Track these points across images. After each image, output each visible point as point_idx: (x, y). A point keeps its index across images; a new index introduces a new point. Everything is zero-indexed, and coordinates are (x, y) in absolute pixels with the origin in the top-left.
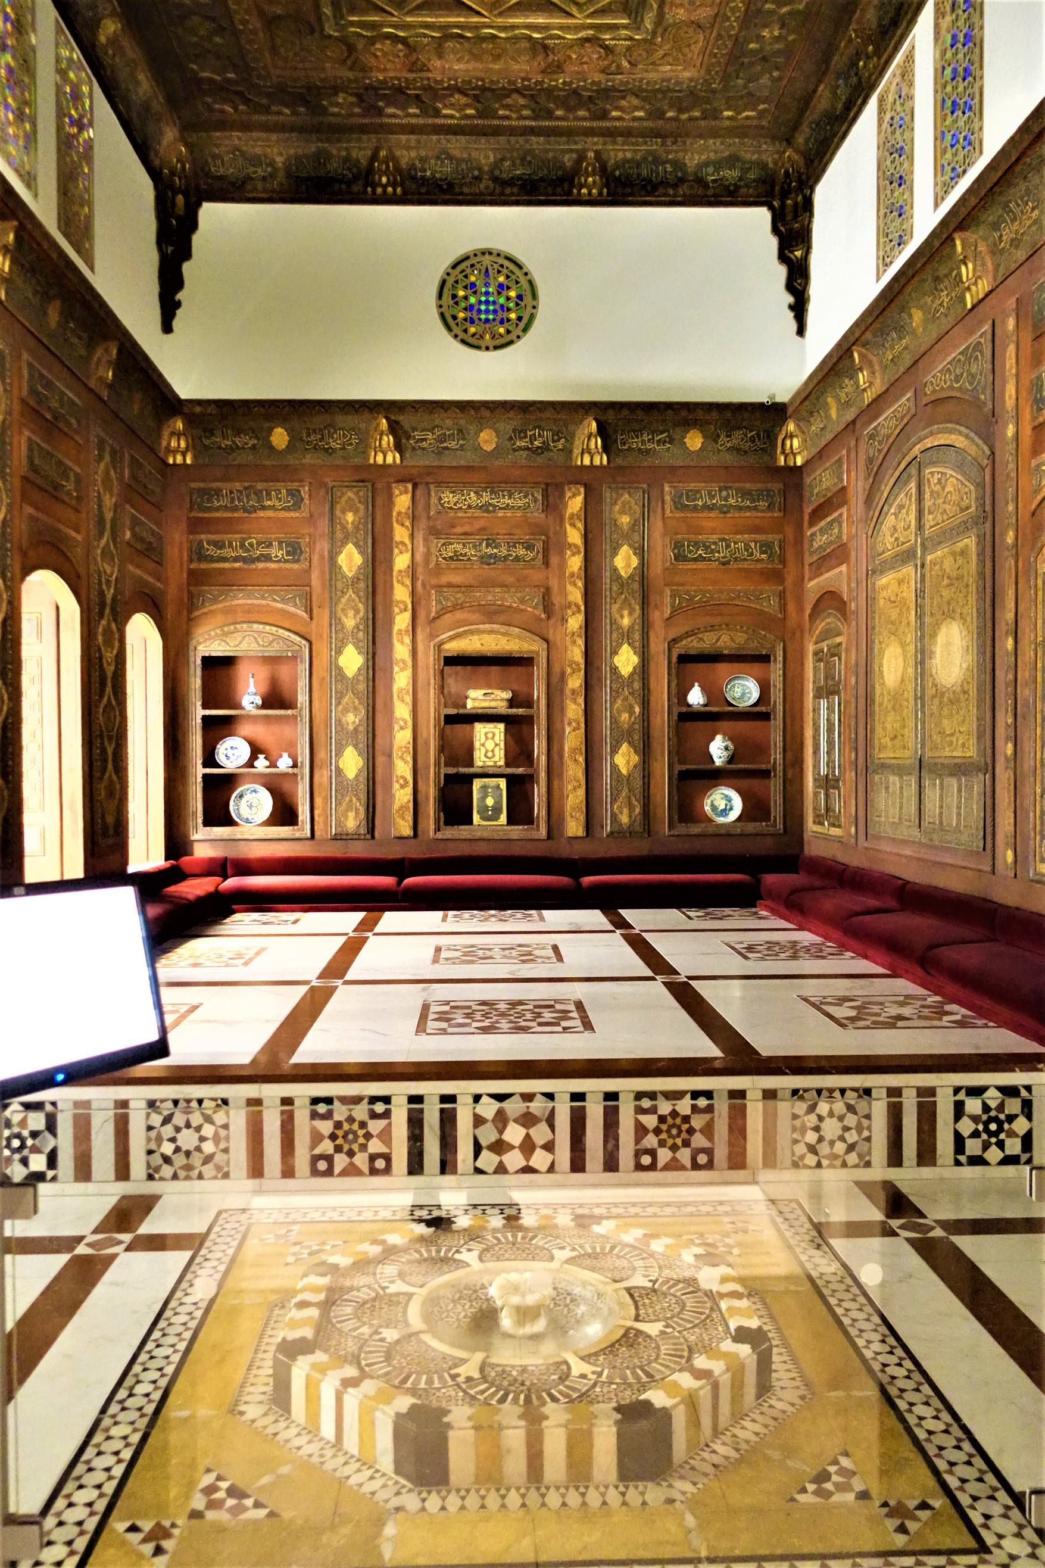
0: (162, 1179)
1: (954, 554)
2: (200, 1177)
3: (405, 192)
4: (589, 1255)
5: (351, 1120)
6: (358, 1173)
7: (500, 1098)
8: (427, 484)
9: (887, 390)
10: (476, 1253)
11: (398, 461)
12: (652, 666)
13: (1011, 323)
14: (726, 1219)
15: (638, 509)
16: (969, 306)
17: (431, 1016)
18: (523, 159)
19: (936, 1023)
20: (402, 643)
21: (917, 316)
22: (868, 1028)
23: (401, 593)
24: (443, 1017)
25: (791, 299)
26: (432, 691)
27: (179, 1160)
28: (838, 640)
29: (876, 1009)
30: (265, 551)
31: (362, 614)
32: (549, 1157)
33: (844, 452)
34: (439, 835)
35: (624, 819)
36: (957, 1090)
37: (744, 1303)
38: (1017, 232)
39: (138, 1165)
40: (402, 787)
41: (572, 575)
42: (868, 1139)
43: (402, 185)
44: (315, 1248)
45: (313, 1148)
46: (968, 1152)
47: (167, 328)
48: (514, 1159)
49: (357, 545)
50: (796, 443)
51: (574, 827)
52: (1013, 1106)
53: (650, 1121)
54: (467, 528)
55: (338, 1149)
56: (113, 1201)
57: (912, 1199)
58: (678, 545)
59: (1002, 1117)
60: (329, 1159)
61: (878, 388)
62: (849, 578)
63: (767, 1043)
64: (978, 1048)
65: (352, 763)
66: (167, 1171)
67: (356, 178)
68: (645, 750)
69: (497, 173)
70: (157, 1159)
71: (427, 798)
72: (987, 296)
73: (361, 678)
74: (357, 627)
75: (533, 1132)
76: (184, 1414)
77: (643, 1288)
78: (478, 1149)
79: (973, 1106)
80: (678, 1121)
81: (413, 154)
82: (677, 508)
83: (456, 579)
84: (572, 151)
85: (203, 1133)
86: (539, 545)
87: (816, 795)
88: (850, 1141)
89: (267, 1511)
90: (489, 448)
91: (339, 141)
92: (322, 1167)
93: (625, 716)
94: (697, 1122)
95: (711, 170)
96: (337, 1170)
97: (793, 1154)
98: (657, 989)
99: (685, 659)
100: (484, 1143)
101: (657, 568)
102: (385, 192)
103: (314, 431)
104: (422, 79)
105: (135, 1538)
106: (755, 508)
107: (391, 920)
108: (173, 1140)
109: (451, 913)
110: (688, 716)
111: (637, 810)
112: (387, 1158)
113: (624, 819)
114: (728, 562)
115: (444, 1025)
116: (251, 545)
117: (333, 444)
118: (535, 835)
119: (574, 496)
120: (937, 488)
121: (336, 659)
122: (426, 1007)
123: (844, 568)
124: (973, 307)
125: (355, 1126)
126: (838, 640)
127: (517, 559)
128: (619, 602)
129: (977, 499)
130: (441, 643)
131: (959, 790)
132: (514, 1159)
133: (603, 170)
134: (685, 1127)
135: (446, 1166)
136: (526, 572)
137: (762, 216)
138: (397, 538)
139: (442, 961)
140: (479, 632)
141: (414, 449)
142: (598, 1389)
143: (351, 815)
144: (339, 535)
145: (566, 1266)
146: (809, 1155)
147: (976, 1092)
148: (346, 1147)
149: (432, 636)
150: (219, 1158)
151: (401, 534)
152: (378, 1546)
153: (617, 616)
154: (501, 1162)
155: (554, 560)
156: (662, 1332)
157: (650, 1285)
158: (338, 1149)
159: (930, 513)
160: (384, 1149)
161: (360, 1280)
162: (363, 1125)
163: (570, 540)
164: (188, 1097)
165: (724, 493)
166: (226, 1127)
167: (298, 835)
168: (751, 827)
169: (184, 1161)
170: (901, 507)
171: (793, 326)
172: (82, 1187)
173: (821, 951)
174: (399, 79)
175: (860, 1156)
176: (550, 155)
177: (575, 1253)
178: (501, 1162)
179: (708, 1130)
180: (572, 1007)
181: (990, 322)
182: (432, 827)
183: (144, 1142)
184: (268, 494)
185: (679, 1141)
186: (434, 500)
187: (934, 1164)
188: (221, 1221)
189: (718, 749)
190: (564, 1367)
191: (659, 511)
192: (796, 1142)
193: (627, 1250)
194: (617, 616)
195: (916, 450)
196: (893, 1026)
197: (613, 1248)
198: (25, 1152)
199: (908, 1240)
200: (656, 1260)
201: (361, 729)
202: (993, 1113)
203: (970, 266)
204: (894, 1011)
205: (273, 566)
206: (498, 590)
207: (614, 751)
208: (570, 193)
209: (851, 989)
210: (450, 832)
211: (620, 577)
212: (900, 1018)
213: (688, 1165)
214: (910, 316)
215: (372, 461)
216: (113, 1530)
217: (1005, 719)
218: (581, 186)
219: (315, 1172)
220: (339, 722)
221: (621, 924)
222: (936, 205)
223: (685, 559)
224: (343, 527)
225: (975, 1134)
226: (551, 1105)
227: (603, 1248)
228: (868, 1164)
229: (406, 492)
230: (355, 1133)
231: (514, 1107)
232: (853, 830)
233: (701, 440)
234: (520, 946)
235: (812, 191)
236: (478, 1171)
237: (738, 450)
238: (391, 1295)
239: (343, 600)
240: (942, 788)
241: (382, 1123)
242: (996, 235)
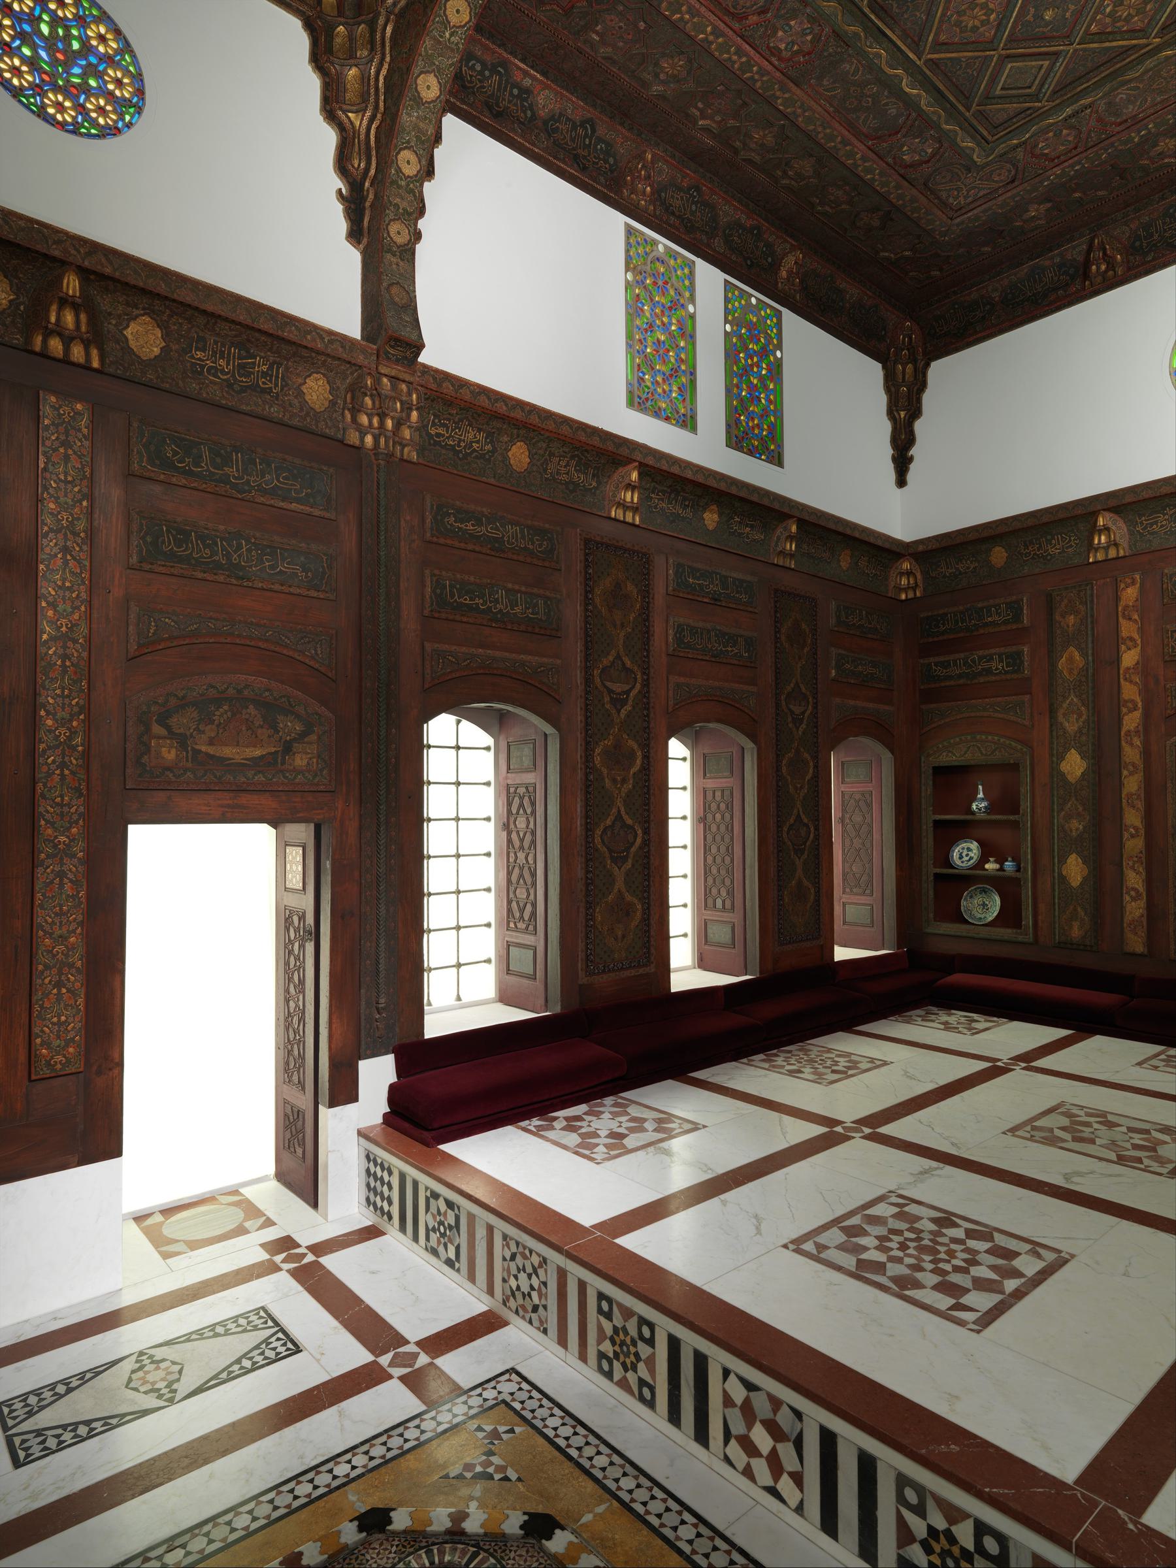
31: (1084, 717)
40: (1134, 899)
47: (901, 482)
65: (1075, 870)
74: (1080, 730)
116: (973, 661)
138: (1124, 633)
143: (1076, 925)
167: (1020, 938)
174: (1079, 163)
205: (994, 678)
239: (1065, 705)
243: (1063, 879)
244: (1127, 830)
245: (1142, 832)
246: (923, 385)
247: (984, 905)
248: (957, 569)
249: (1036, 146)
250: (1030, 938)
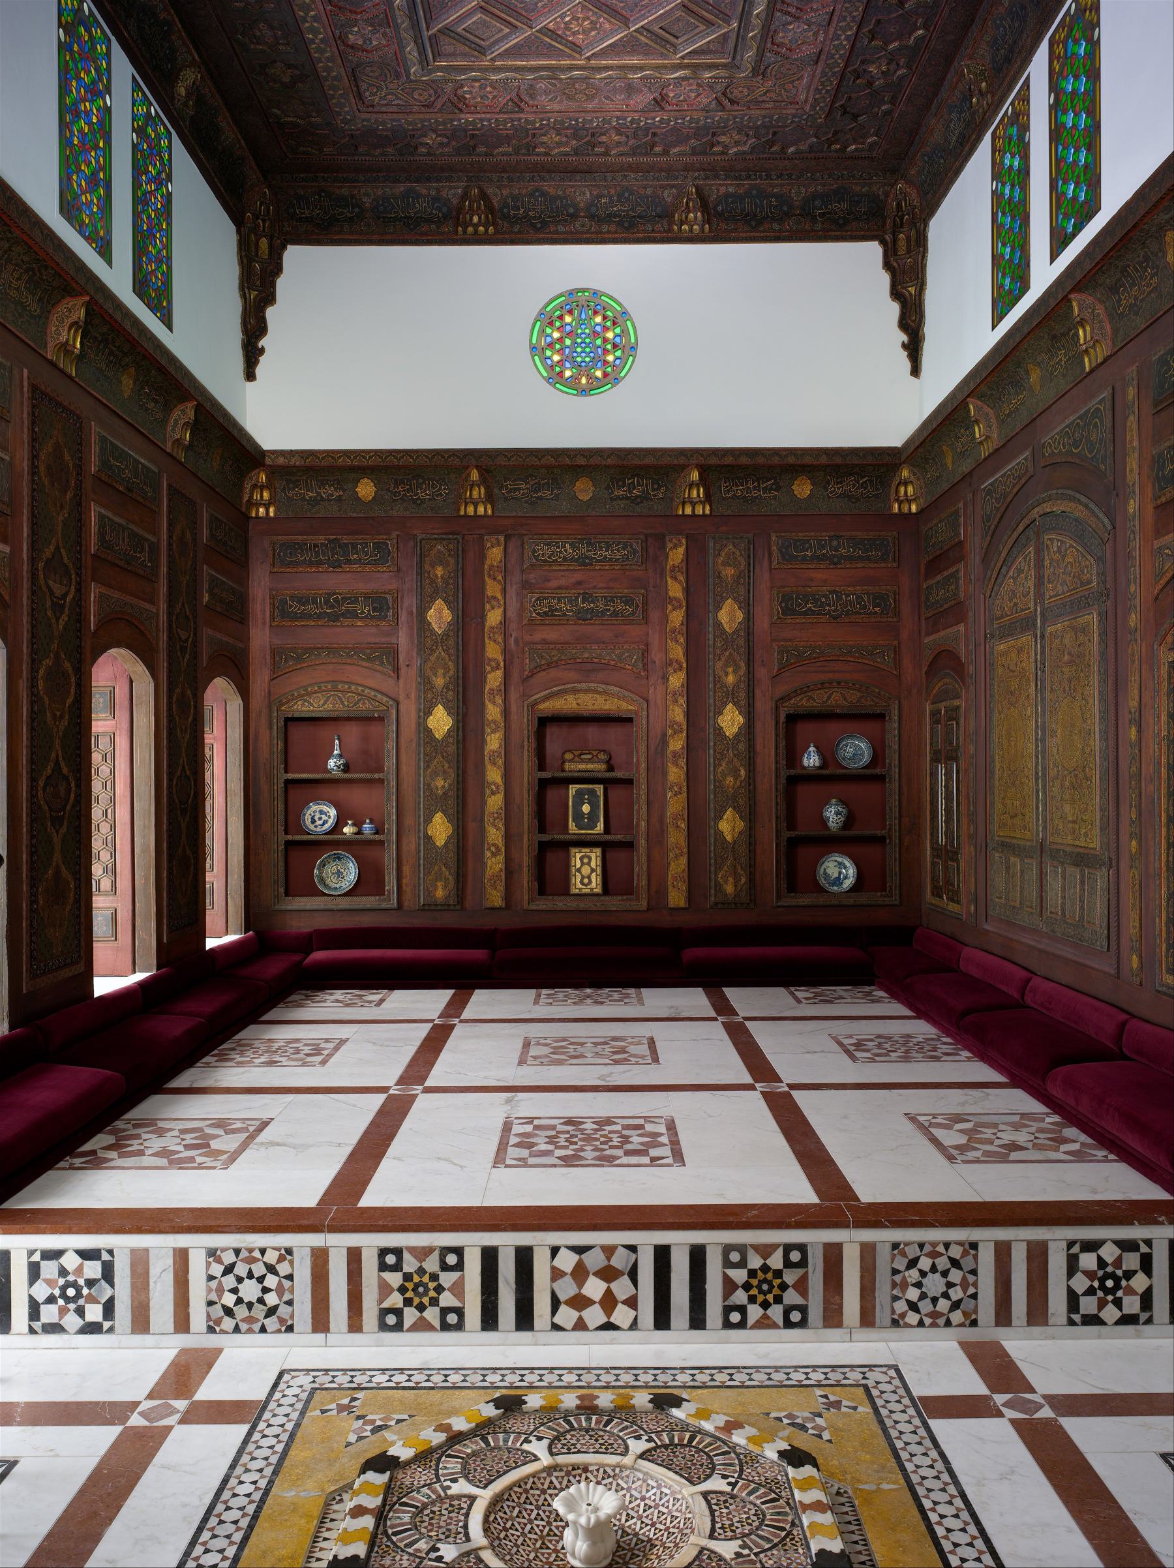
0: (223, 1332)
1: (1074, 629)
2: (263, 1330)
3: (496, 232)
4: (666, 1447)
5: (421, 1271)
6: (431, 1328)
7: (580, 1250)
8: (521, 536)
9: (1004, 445)
10: (546, 1442)
11: (490, 512)
12: (759, 726)
13: (1131, 392)
14: (819, 1392)
15: (743, 562)
16: (1087, 369)
17: (513, 1140)
18: (620, 196)
19: (1053, 1155)
20: (494, 703)
21: (1035, 376)
22: (978, 1161)
23: (493, 651)
24: (526, 1143)
25: (904, 338)
26: (526, 753)
27: (241, 1312)
28: (956, 703)
29: (988, 1133)
30: (351, 607)
31: (451, 672)
32: (633, 1313)
33: (961, 505)
34: (533, 907)
35: (729, 889)
36: (1071, 1244)
37: (827, 1518)
38: (1136, 298)
39: (198, 1315)
40: (494, 855)
41: (674, 631)
42: (974, 1296)
43: (494, 224)
44: (379, 1423)
45: (381, 1301)
46: (1082, 1312)
48: (594, 1316)
49: (446, 601)
50: (910, 490)
51: (676, 897)
52: (1132, 1261)
53: (739, 1275)
54: (562, 582)
55: (408, 1302)
56: (169, 1355)
57: (1020, 1364)
58: (786, 598)
59: (1119, 1273)
60: (398, 1313)
61: (996, 441)
62: (967, 639)
63: (870, 1184)
64: (1095, 1192)
65: (440, 829)
66: (228, 1323)
67: (445, 217)
68: (751, 816)
69: (593, 209)
70: (218, 1311)
71: (521, 867)
72: (1105, 360)
73: (451, 740)
74: (446, 686)
75: (615, 1286)
77: (722, 1493)
78: (555, 1304)
79: (1088, 1261)
80: (769, 1276)
81: (506, 192)
82: (784, 558)
83: (551, 634)
84: (672, 186)
85: (267, 1283)
86: (638, 600)
87: (934, 864)
88: (954, 1298)
90: (585, 497)
91: (429, 180)
92: (391, 1321)
93: (730, 780)
94: (790, 1277)
95: (818, 203)
96: (406, 1325)
97: (893, 1312)
98: (754, 1103)
99: (793, 719)
100: (562, 1297)
101: (763, 623)
102: (476, 231)
103: (402, 482)
104: (512, 120)
106: (868, 559)
107: (482, 1001)
108: (235, 1291)
109: (545, 991)
110: (796, 780)
111: (743, 880)
112: (460, 1312)
113: (729, 889)
114: (840, 616)
115: (524, 1153)
116: (336, 600)
117: (421, 495)
118: (634, 905)
119: (675, 547)
120: (1056, 557)
121: (425, 720)
122: (507, 1127)
123: (961, 627)
124: (1092, 371)
125: (426, 1279)
126: (956, 703)
127: (615, 614)
128: (723, 659)
129: (1098, 574)
130: (536, 703)
131: (1082, 883)
132: (594, 1316)
133: (704, 206)
134: (776, 1282)
135: (525, 1320)
136: (625, 627)
137: (873, 251)
139: (530, 1060)
140: (574, 691)
141: (506, 499)
143: (440, 884)
144: (428, 590)
145: (640, 1461)
146: (910, 1313)
147: (1091, 1246)
148: (416, 1301)
149: (525, 696)
150: (284, 1311)
151: (492, 588)
153: (722, 674)
154: (580, 1318)
155: (654, 616)
156: (738, 1555)
157: (728, 1489)
158: (408, 1302)
159: (1049, 582)
160: (456, 1303)
161: (422, 1475)
162: (434, 1277)
163: (671, 593)
164: (251, 1246)
165: (835, 543)
166: (290, 1277)
167: (384, 905)
168: (863, 898)
169: (246, 1313)
170: (1020, 571)
171: (907, 365)
172: (138, 1339)
173: (935, 1049)
174: (489, 120)
175: (965, 1314)
176: (649, 191)
177: (652, 1445)
178: (580, 1318)
179: (802, 1286)
180: (662, 1129)
181: (1110, 388)
182: (526, 897)
183: (204, 1294)
184: (354, 546)
185: (770, 1297)
186: (527, 553)
187: (1046, 1323)
188: (282, 1386)
189: (833, 815)
191: (766, 564)
192: (895, 1298)
193: (708, 1440)
194: (722, 674)
195: (1035, 513)
196: (1003, 1159)
197: (692, 1439)
198: (81, 1302)
199: (1013, 1422)
200: (738, 1455)
201: (451, 793)
202: (1109, 1269)
203: (1088, 328)
204: (1007, 1137)
206: (595, 647)
207: (719, 817)
208: (670, 230)
209: (963, 1104)
210: (543, 904)
211: (724, 632)
212: (1014, 1147)
213: (781, 1322)
214: (1027, 373)
215: (462, 513)
217: (1129, 814)
218: (682, 223)
219: (383, 1327)
220: (428, 787)
221: (723, 1008)
222: (1053, 259)
223: (793, 612)
224: (433, 582)
225: (1090, 1291)
226: (634, 1256)
227: (681, 1439)
228: (974, 1323)
229: (498, 545)
230: (425, 1286)
231: (595, 1260)
232: (972, 908)
233: (810, 487)
234: (615, 1039)
235: (926, 226)
236: (556, 1327)
237: (850, 497)
238: (452, 1498)
240: (1064, 878)
241: (455, 1275)
242: (1115, 298)
243: (428, 839)
244: (489, 787)
245: (502, 788)
246: (278, 269)
247: (339, 873)
248: (318, 494)
249: (462, 87)
250: (394, 903)
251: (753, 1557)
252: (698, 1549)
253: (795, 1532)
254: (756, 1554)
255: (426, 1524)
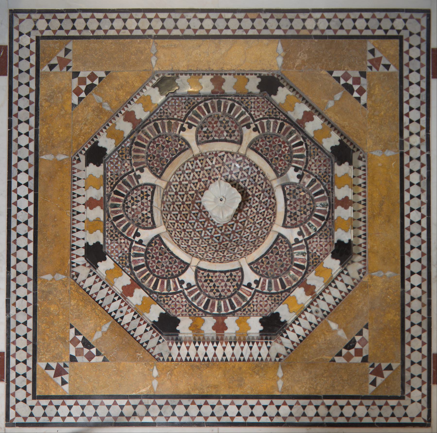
4: (173, 277)
76: (389, 153)
89: (333, 75)
105: (385, 61)
142: (184, 114)
152: (284, 51)
156: (142, 170)
190: (199, 139)
200: (130, 267)
216: (395, 66)
251: (135, 168)
252: (162, 178)
253: (109, 189)
254: (133, 171)
255: (308, 202)
